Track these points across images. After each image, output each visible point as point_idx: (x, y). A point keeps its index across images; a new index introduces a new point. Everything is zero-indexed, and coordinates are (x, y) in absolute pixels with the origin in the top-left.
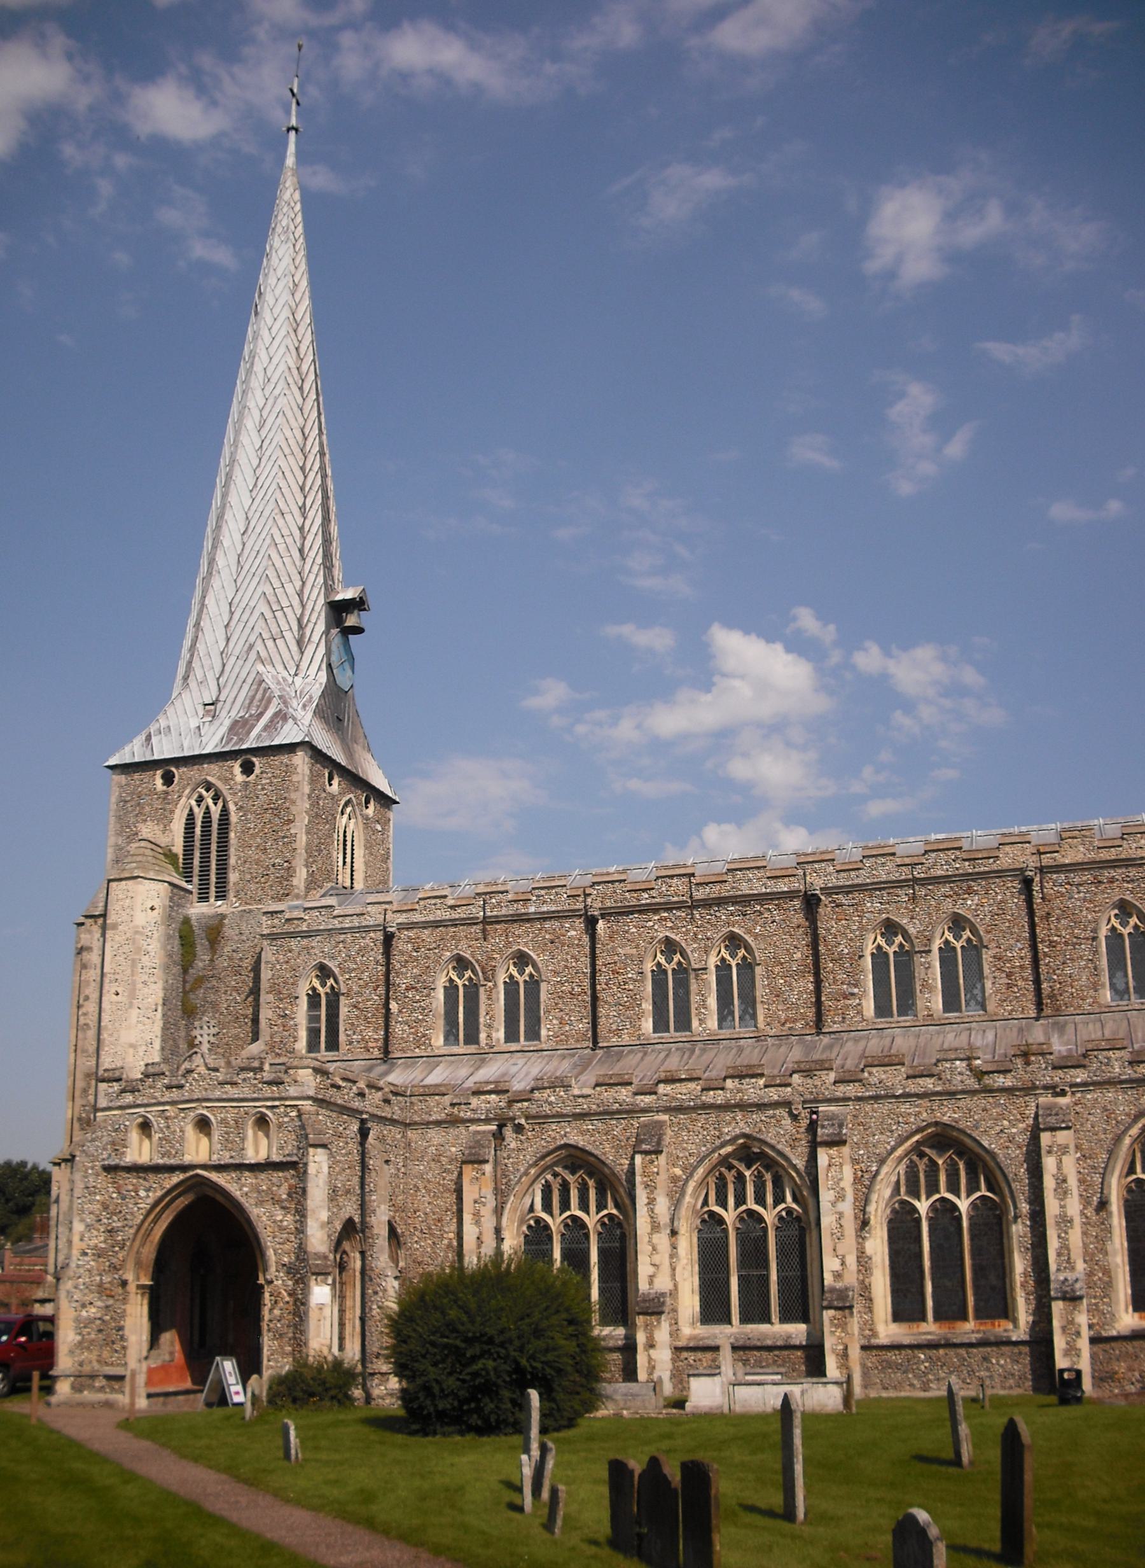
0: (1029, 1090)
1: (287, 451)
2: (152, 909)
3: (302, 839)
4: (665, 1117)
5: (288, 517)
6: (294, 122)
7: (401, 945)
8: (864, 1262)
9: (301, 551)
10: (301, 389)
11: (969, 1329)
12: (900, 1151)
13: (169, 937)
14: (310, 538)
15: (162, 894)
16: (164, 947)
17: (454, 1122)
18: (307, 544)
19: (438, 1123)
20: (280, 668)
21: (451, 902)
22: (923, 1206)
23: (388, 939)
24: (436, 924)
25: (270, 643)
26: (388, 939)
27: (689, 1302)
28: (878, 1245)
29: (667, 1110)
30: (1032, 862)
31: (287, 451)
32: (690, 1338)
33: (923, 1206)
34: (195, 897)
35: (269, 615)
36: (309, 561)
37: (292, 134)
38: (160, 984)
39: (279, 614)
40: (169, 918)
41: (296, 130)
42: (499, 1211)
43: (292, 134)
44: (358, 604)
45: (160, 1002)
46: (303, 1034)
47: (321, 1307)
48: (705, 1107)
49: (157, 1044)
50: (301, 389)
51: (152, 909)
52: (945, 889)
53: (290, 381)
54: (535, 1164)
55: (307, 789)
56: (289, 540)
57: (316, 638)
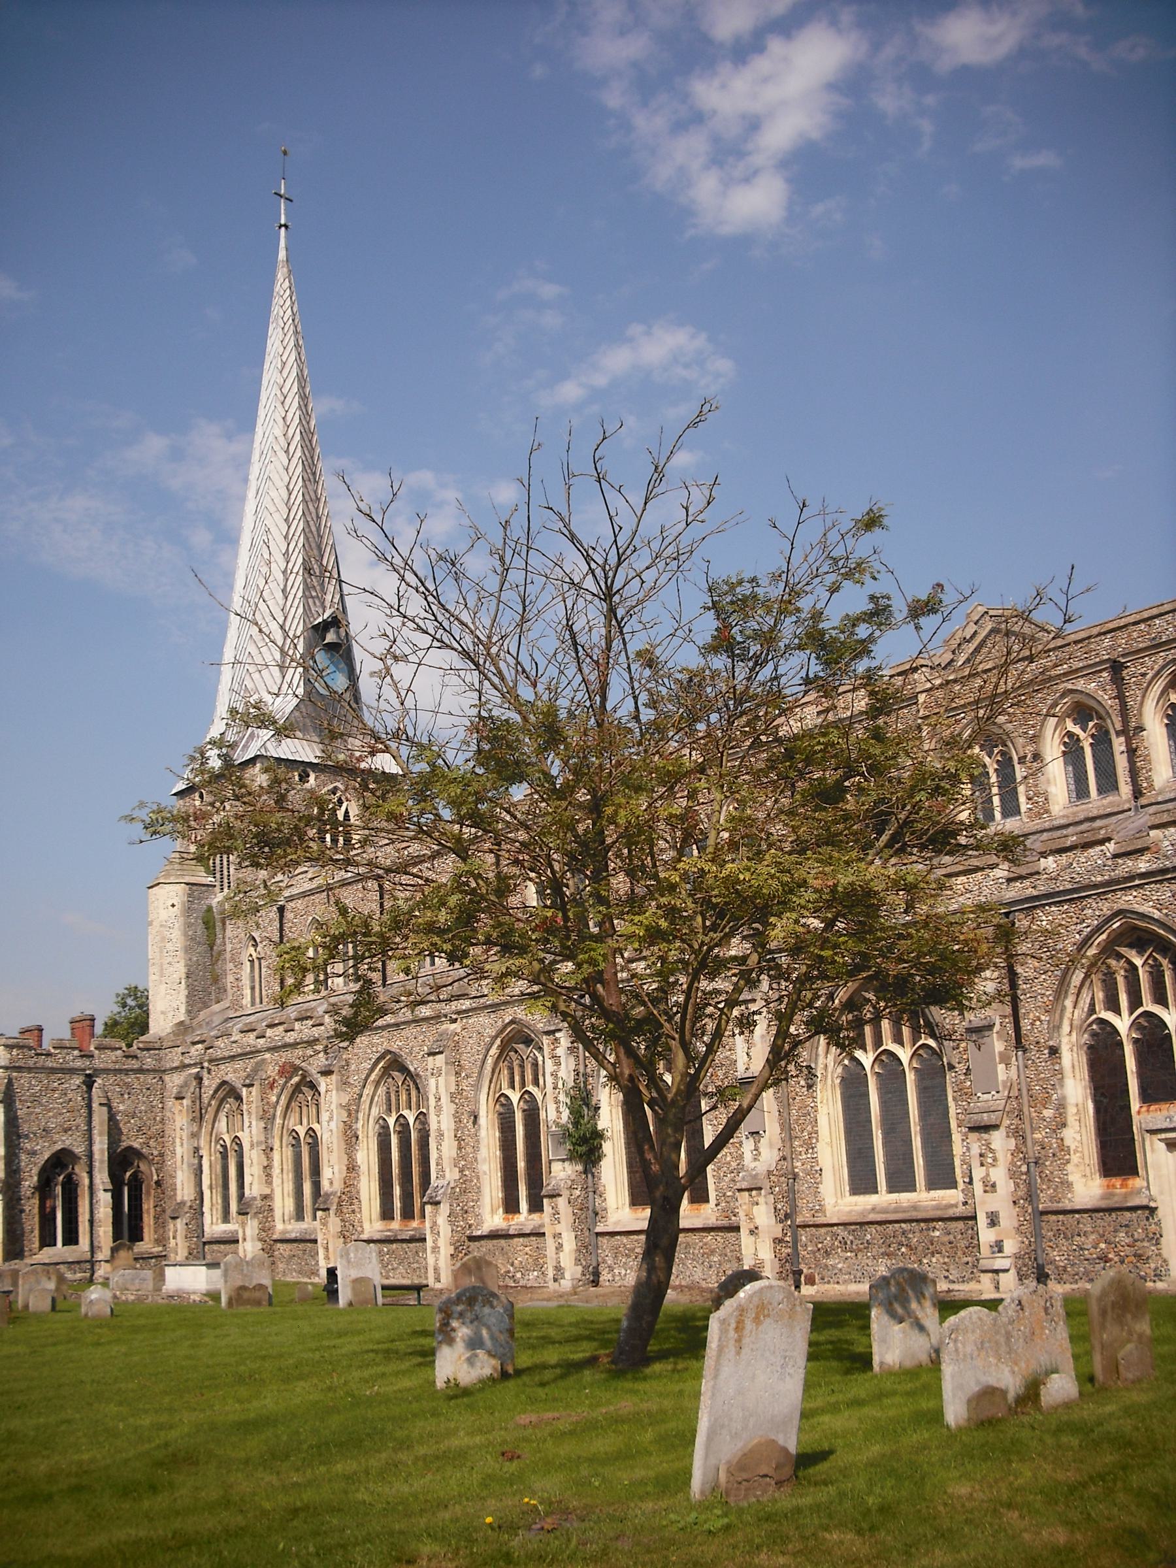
0: (437, 1018)
1: (272, 509)
2: (173, 906)
4: (268, 1056)
6: (283, 222)
7: (289, 915)
8: (352, 1168)
9: (283, 591)
10: (287, 452)
11: (396, 1225)
12: (373, 1077)
13: (189, 925)
15: (180, 893)
16: (185, 934)
17: (185, 1066)
18: (290, 584)
19: (176, 1068)
21: (310, 875)
22: (391, 1121)
23: (281, 910)
24: (304, 895)
25: (256, 676)
26: (281, 910)
27: (283, 1204)
28: (367, 1156)
29: (269, 1049)
31: (272, 509)
32: (284, 1232)
33: (391, 1121)
34: (217, 889)
35: (254, 652)
36: (291, 598)
37: (283, 229)
38: (182, 963)
39: (263, 650)
40: (188, 910)
41: (286, 226)
42: (195, 1135)
43: (283, 229)
44: (334, 622)
45: (184, 976)
46: (247, 992)
48: (286, 1046)
49: (183, 1009)
50: (287, 452)
51: (173, 906)
53: (276, 448)
54: (213, 1097)
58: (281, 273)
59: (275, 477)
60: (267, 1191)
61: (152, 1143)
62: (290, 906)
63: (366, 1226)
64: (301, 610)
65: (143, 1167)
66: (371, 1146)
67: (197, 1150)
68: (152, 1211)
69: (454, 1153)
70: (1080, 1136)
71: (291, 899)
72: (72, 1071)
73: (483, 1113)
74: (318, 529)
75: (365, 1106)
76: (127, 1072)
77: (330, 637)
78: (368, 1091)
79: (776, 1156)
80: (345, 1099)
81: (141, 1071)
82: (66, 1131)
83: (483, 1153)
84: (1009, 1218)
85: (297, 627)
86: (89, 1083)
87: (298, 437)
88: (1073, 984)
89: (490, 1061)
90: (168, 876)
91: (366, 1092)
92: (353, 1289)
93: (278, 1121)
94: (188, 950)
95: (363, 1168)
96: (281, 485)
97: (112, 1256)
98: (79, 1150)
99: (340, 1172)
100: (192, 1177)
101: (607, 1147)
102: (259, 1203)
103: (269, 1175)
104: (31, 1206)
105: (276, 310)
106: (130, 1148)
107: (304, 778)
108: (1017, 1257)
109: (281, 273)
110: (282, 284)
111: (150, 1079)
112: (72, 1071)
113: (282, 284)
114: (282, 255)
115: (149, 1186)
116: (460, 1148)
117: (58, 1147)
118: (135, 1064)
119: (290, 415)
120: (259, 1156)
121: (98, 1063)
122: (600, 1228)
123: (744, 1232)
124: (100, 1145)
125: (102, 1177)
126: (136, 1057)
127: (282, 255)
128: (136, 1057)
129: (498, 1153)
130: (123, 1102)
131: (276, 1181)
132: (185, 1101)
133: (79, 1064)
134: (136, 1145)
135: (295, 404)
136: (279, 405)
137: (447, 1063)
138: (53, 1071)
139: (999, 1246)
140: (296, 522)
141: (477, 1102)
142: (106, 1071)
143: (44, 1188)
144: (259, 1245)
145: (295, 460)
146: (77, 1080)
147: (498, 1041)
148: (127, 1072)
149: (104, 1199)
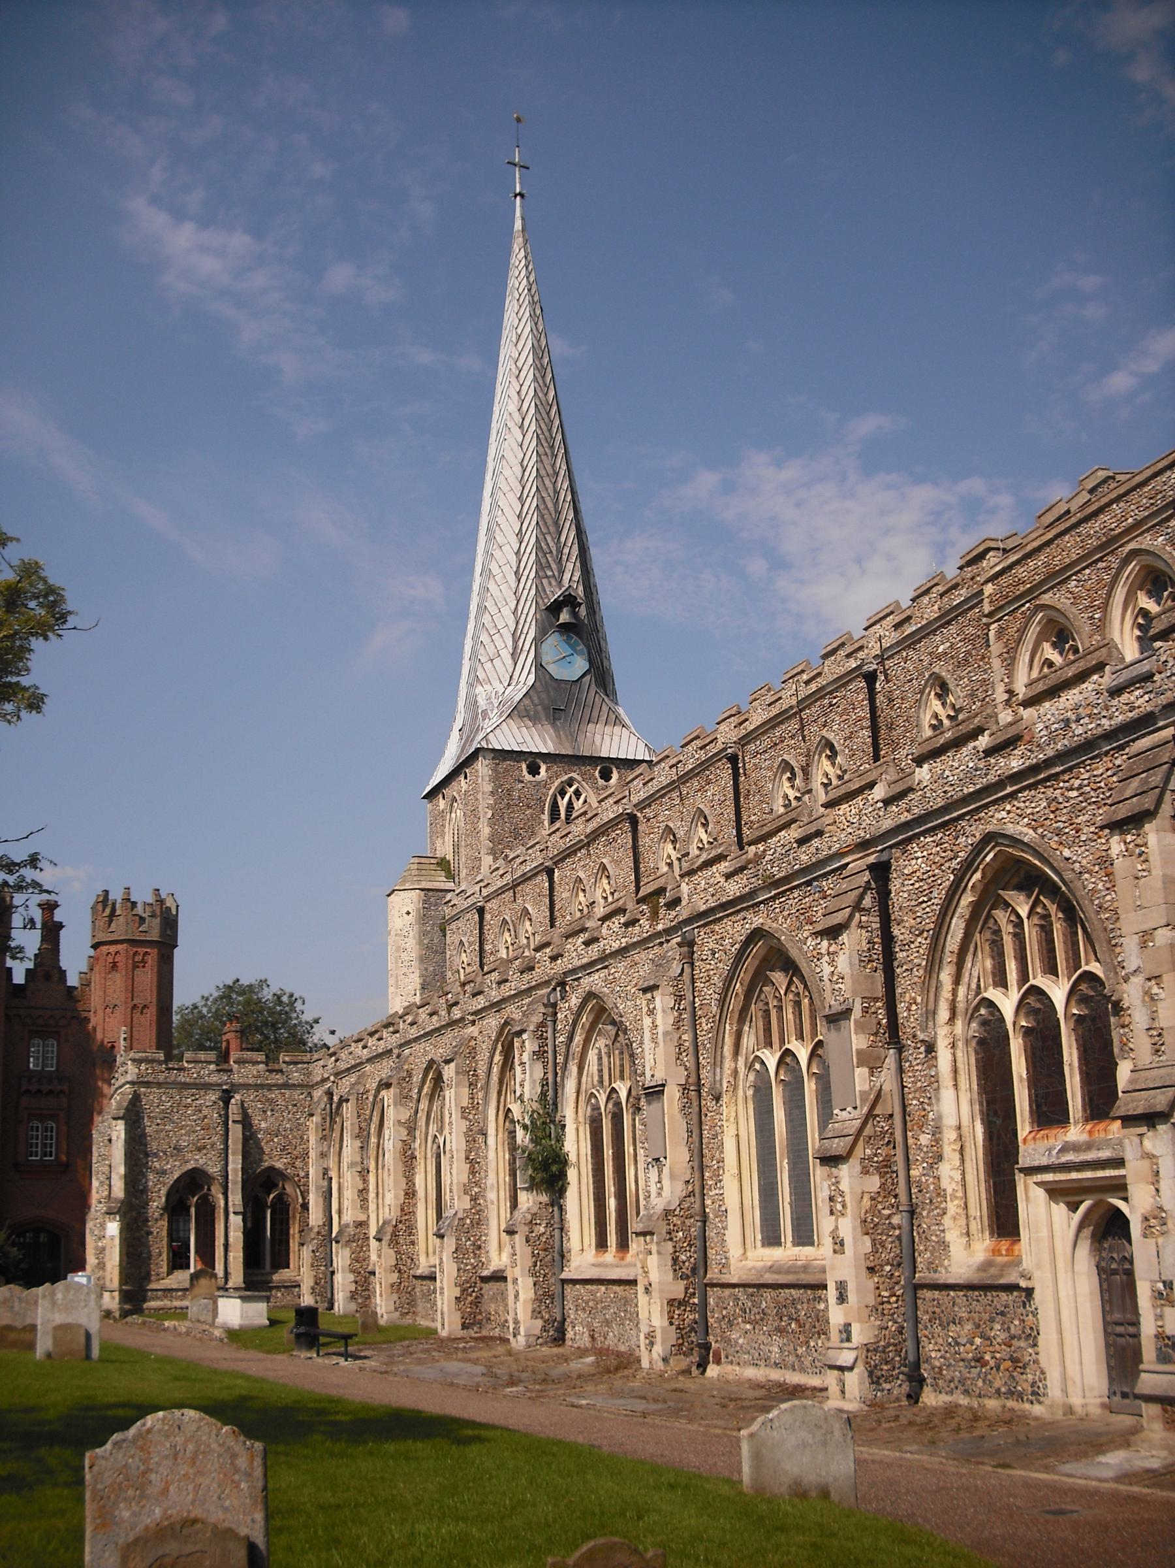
2: (408, 913)
3: (486, 831)
5: (506, 548)
7: (488, 917)
8: (410, 1193)
10: (521, 427)
12: (425, 1090)
13: (424, 933)
14: (525, 559)
15: (415, 900)
16: (420, 943)
20: (496, 684)
25: (488, 665)
30: (734, 735)
37: (518, 198)
41: (522, 195)
42: (323, 1155)
43: (518, 198)
45: (419, 987)
47: (112, 1238)
50: (521, 427)
51: (408, 913)
52: (695, 783)
55: (488, 788)
56: (506, 568)
57: (526, 647)
58: (518, 243)
59: (508, 455)
60: (363, 1218)
61: (298, 1163)
62: (488, 906)
63: (422, 1259)
64: (533, 592)
65: (289, 1189)
66: (429, 1169)
67: (326, 1171)
68: (297, 1236)
69: (464, 1178)
70: (959, 1175)
71: (488, 899)
72: (207, 1087)
73: (491, 1131)
74: (556, 503)
75: (422, 1122)
76: (269, 1087)
77: (565, 617)
78: (424, 1105)
79: (680, 1189)
80: (405, 1114)
81: (286, 1086)
82: (199, 1149)
83: (491, 1179)
84: (862, 1289)
85: (530, 612)
86: (226, 1097)
87: (532, 410)
88: (948, 949)
89: (495, 1070)
90: (404, 882)
91: (421, 1106)
92: (55, 1337)
93: (373, 1140)
94: (422, 959)
95: (421, 1193)
96: (515, 462)
97: (192, 1284)
98: (214, 1170)
99: (396, 1197)
100: (321, 1200)
101: (572, 1174)
102: (351, 1230)
103: (365, 1200)
104: (159, 1229)
105: (512, 283)
106: (271, 1168)
107: (534, 770)
108: (869, 1349)
109: (518, 243)
110: (518, 256)
111: (296, 1094)
112: (207, 1087)
113: (518, 256)
114: (518, 225)
115: (294, 1208)
116: (473, 1172)
117: (189, 1166)
118: (279, 1079)
119: (525, 388)
120: (353, 1177)
121: (236, 1078)
122: (564, 1276)
123: (640, 1288)
124: (235, 1163)
125: (236, 1198)
126: (281, 1071)
127: (518, 225)
128: (281, 1071)
129: (507, 1179)
130: (265, 1120)
131: (372, 1206)
132: (314, 1118)
133: (215, 1078)
134: (279, 1165)
135: (531, 376)
136: (513, 380)
137: (457, 1073)
138: (185, 1086)
139: (846, 1330)
140: (529, 499)
141: (486, 1118)
142: (246, 1086)
143: (176, 1208)
144: (352, 1277)
145: (529, 434)
146: (213, 1096)
147: (499, 1047)
148: (269, 1087)
149: (236, 1221)
